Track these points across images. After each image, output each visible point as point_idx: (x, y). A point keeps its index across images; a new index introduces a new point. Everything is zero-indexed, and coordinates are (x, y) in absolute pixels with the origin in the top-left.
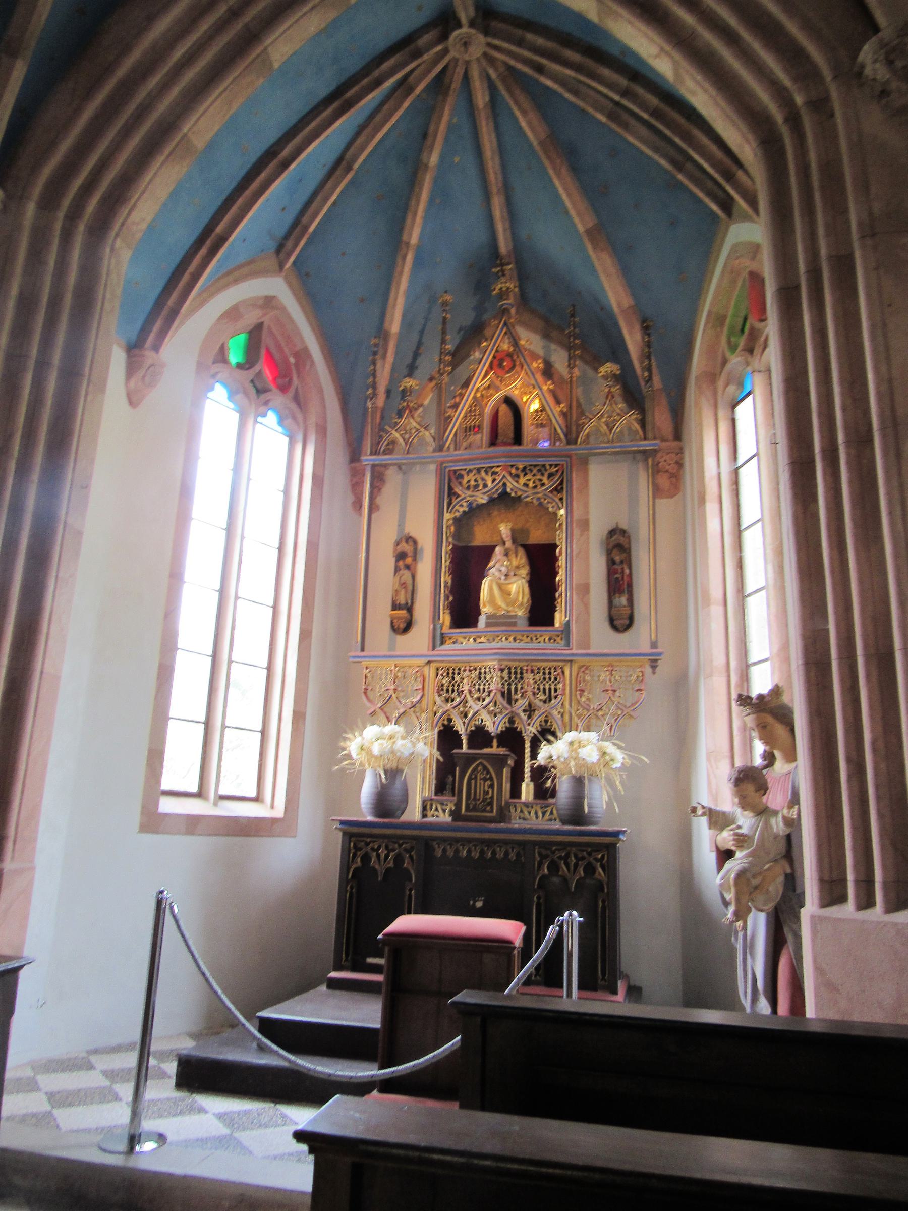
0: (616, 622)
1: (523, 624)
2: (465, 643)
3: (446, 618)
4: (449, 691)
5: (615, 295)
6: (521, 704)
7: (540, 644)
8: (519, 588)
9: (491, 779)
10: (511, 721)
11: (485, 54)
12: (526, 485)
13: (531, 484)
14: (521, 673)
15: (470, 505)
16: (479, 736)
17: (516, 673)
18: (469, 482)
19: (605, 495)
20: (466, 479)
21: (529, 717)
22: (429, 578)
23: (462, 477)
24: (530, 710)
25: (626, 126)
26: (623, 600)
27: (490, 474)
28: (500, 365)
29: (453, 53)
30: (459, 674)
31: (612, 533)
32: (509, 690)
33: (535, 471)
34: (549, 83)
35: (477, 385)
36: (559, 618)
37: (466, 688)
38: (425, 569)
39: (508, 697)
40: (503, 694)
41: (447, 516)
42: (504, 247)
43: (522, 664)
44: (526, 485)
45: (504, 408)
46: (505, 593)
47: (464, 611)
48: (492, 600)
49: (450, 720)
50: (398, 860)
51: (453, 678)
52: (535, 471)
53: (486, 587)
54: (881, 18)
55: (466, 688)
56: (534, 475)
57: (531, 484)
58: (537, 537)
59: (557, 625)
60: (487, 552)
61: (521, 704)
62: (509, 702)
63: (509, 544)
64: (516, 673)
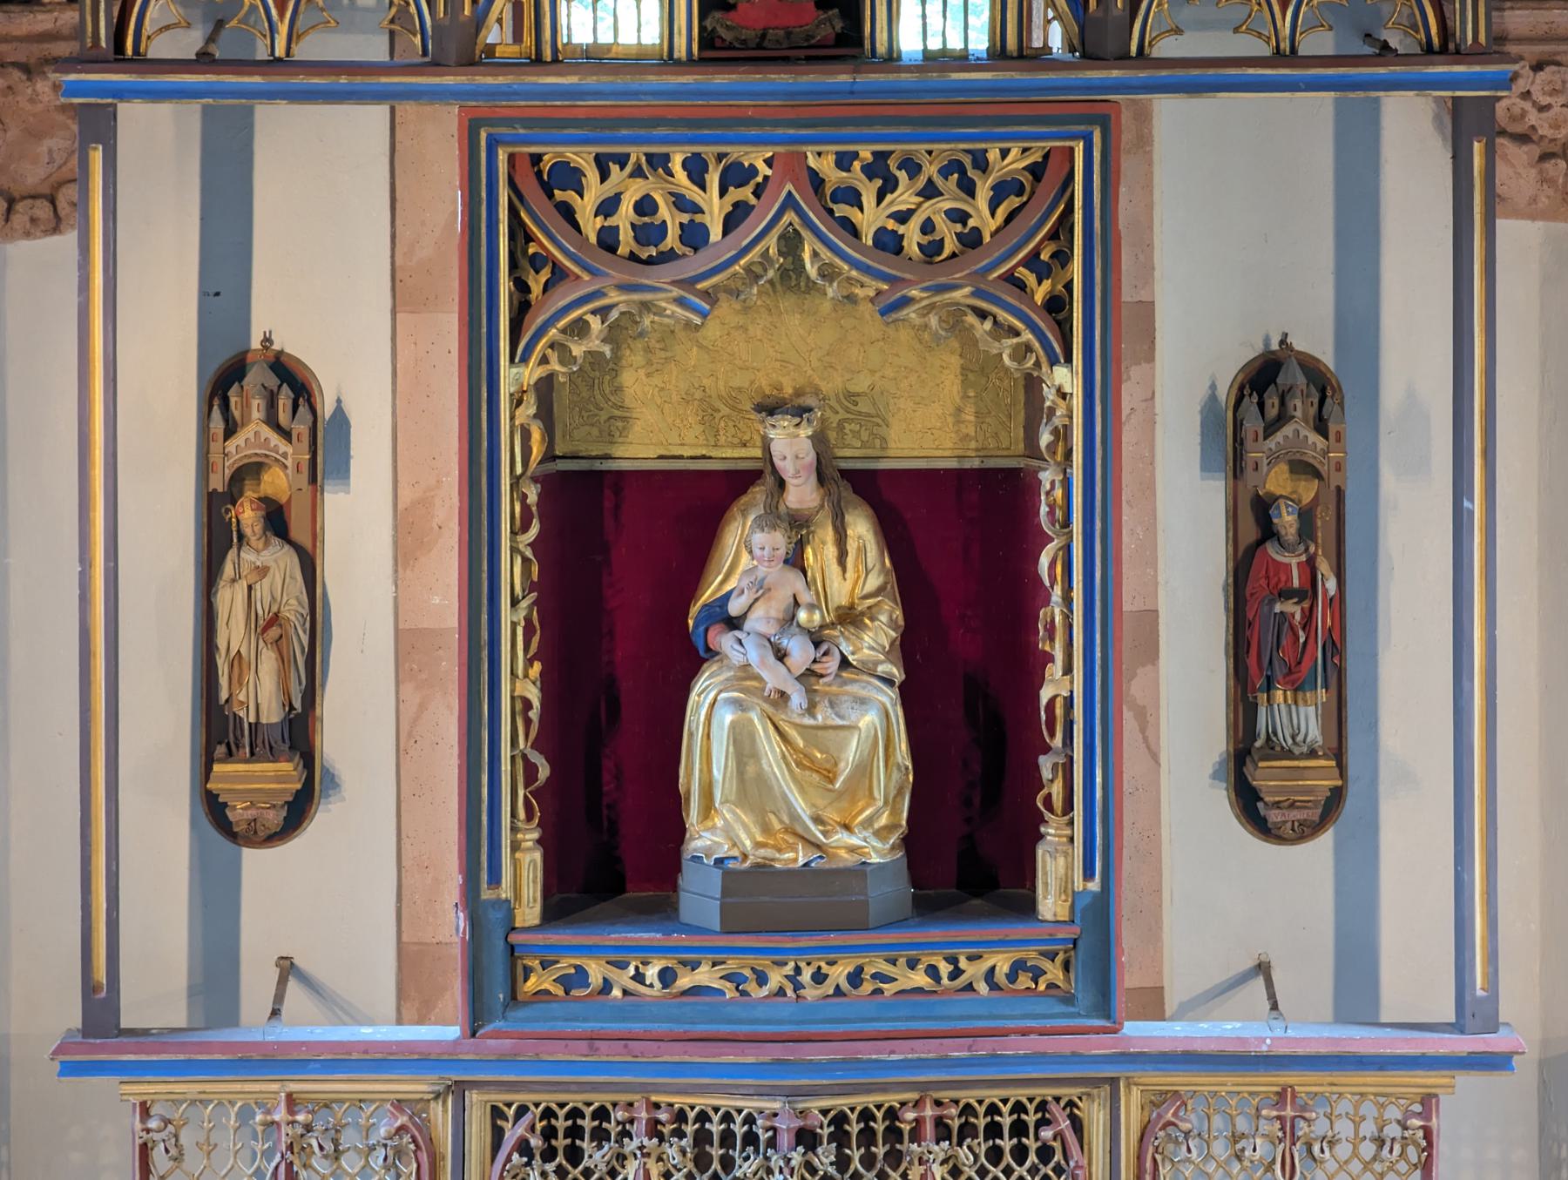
2: (622, 965)
3: (524, 872)
8: (870, 720)
12: (889, 243)
13: (912, 235)
14: (893, 1134)
17: (867, 1137)
18: (608, 207)
27: (713, 179)
30: (600, 1136)
33: (931, 170)
36: (1057, 872)
38: (356, 524)
41: (511, 377)
43: (892, 1099)
44: (889, 243)
46: (816, 767)
47: (604, 819)
48: (753, 790)
51: (574, 1155)
52: (931, 170)
56: (930, 191)
57: (912, 235)
59: (1051, 905)
60: (698, 504)
63: (802, 494)
64: (867, 1137)
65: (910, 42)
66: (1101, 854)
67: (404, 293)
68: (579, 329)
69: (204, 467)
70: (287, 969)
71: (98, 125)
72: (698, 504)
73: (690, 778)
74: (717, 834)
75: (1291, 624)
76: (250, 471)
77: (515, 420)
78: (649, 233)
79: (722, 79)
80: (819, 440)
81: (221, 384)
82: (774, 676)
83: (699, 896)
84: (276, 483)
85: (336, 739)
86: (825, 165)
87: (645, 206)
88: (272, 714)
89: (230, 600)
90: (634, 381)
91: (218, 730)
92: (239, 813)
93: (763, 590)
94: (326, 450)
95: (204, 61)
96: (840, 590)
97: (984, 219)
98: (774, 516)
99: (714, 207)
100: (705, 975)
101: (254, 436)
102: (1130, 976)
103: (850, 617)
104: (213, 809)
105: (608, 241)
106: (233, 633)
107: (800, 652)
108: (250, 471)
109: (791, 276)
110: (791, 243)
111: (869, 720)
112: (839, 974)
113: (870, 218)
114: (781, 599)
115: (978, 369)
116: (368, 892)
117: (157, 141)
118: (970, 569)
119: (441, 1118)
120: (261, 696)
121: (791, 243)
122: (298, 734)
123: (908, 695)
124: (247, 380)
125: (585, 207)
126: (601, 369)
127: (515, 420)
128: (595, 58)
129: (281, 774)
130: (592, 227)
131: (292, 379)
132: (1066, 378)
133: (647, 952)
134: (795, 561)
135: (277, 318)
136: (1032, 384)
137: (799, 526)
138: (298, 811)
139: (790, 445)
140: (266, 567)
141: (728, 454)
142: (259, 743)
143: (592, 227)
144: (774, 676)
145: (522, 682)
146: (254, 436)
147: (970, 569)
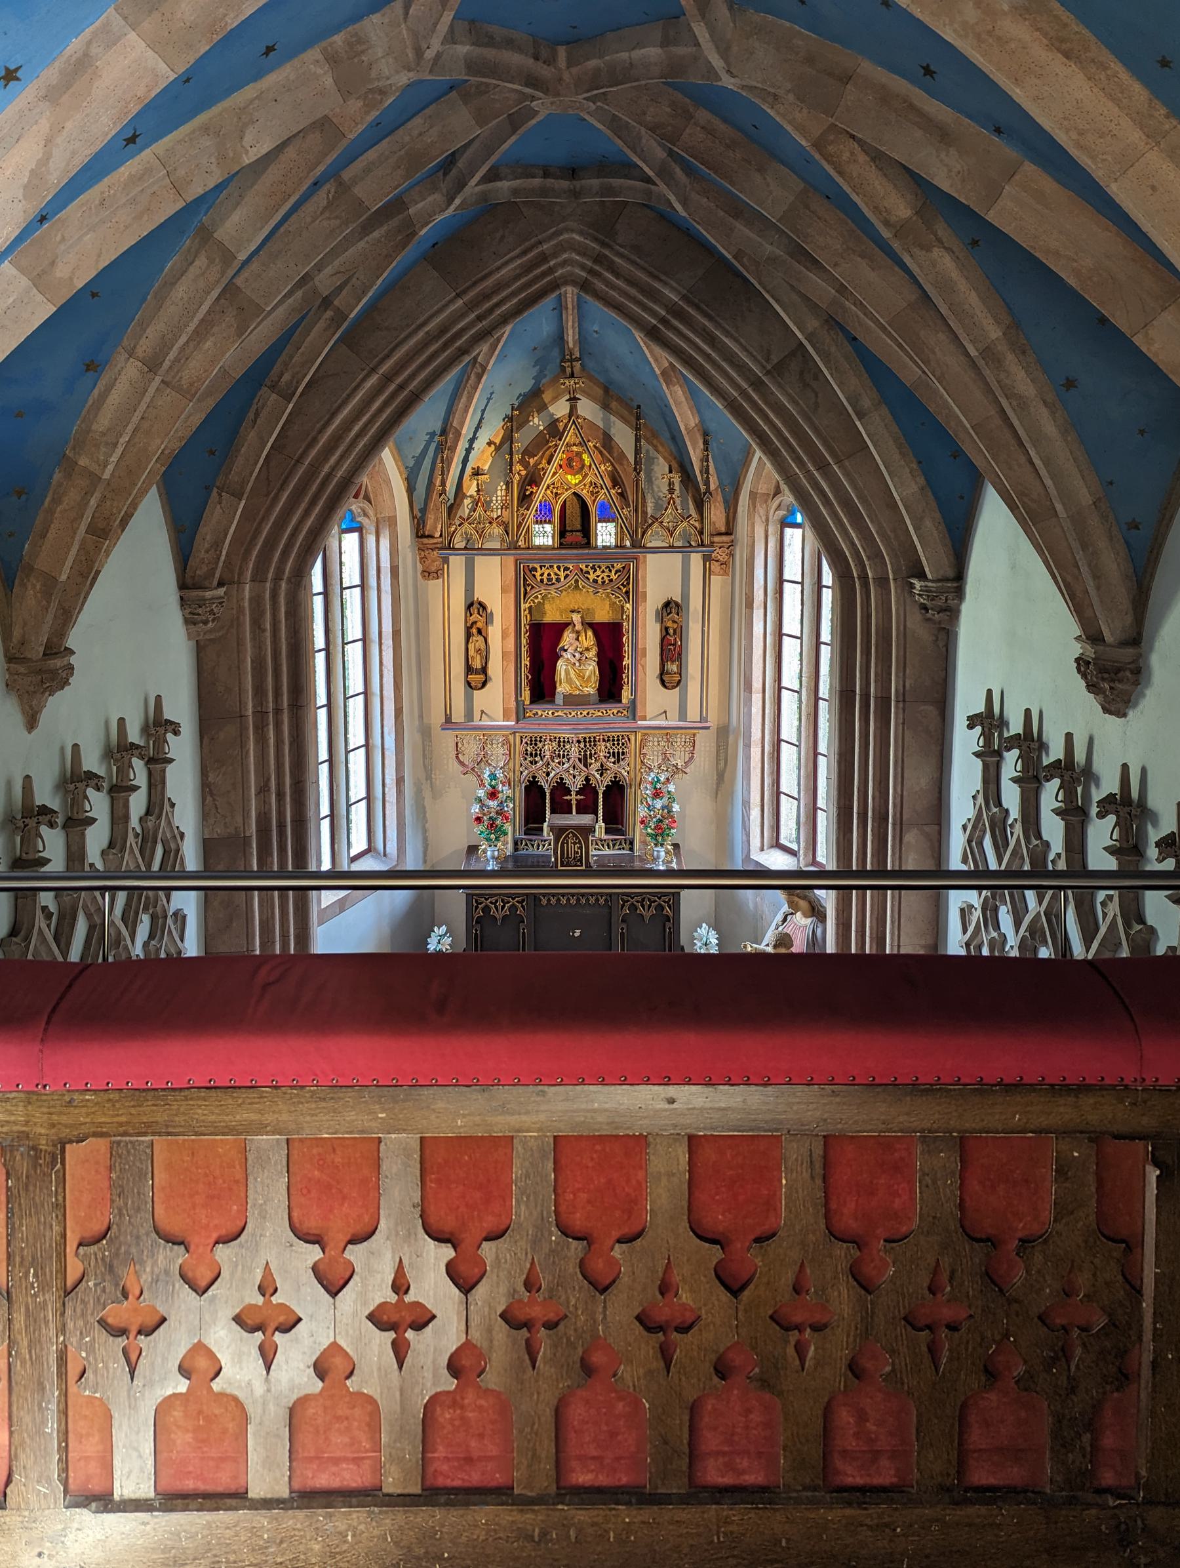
0: (666, 678)
2: (544, 711)
3: (526, 695)
4: (534, 755)
7: (609, 717)
8: (591, 668)
9: (580, 842)
10: (587, 779)
12: (595, 581)
13: (600, 580)
16: (561, 788)
18: (542, 575)
19: (660, 575)
20: (539, 572)
21: (601, 775)
24: (602, 770)
26: (675, 668)
31: (668, 605)
32: (585, 755)
35: (548, 482)
36: (626, 694)
37: (548, 753)
38: (495, 632)
39: (584, 761)
40: (580, 760)
44: (595, 581)
46: (581, 676)
47: (541, 685)
48: (569, 681)
49: (534, 777)
55: (548, 753)
57: (600, 580)
58: (603, 615)
59: (624, 701)
62: (586, 766)
63: (579, 627)
65: (599, 543)
66: (634, 691)
67: (504, 590)
68: (537, 597)
69: (466, 622)
70: (482, 712)
71: (446, 560)
73: (557, 678)
74: (562, 688)
76: (475, 623)
77: (524, 614)
78: (550, 580)
79: (563, 552)
80: (582, 617)
81: (469, 607)
82: (573, 660)
83: (559, 699)
84: (479, 625)
85: (490, 672)
86: (583, 567)
87: (549, 575)
88: (479, 667)
90: (547, 606)
91: (469, 669)
92: (473, 684)
93: (571, 644)
94: (489, 619)
95: (466, 548)
96: (586, 644)
97: (614, 577)
98: (573, 631)
99: (562, 574)
100: (560, 713)
101: (475, 616)
102: (639, 714)
103: (587, 649)
104: (469, 684)
105: (542, 581)
106: (472, 652)
107: (577, 655)
108: (475, 623)
109: (577, 587)
110: (577, 581)
111: (591, 668)
112: (585, 713)
113: (592, 577)
114: (573, 648)
115: (613, 604)
116: (497, 699)
117: (457, 563)
118: (610, 641)
119: (511, 738)
120: (477, 664)
121: (577, 581)
122: (484, 670)
123: (598, 663)
124: (474, 606)
125: (538, 574)
126: (540, 605)
127: (524, 614)
128: (539, 547)
129: (481, 677)
130: (539, 578)
131: (482, 606)
133: (549, 709)
134: (577, 639)
135: (479, 595)
136: (623, 607)
137: (578, 632)
138: (484, 684)
139: (576, 618)
140: (477, 641)
141: (564, 620)
142: (477, 672)
143: (539, 578)
144: (573, 660)
145: (526, 661)
146: (475, 616)
147: (610, 641)
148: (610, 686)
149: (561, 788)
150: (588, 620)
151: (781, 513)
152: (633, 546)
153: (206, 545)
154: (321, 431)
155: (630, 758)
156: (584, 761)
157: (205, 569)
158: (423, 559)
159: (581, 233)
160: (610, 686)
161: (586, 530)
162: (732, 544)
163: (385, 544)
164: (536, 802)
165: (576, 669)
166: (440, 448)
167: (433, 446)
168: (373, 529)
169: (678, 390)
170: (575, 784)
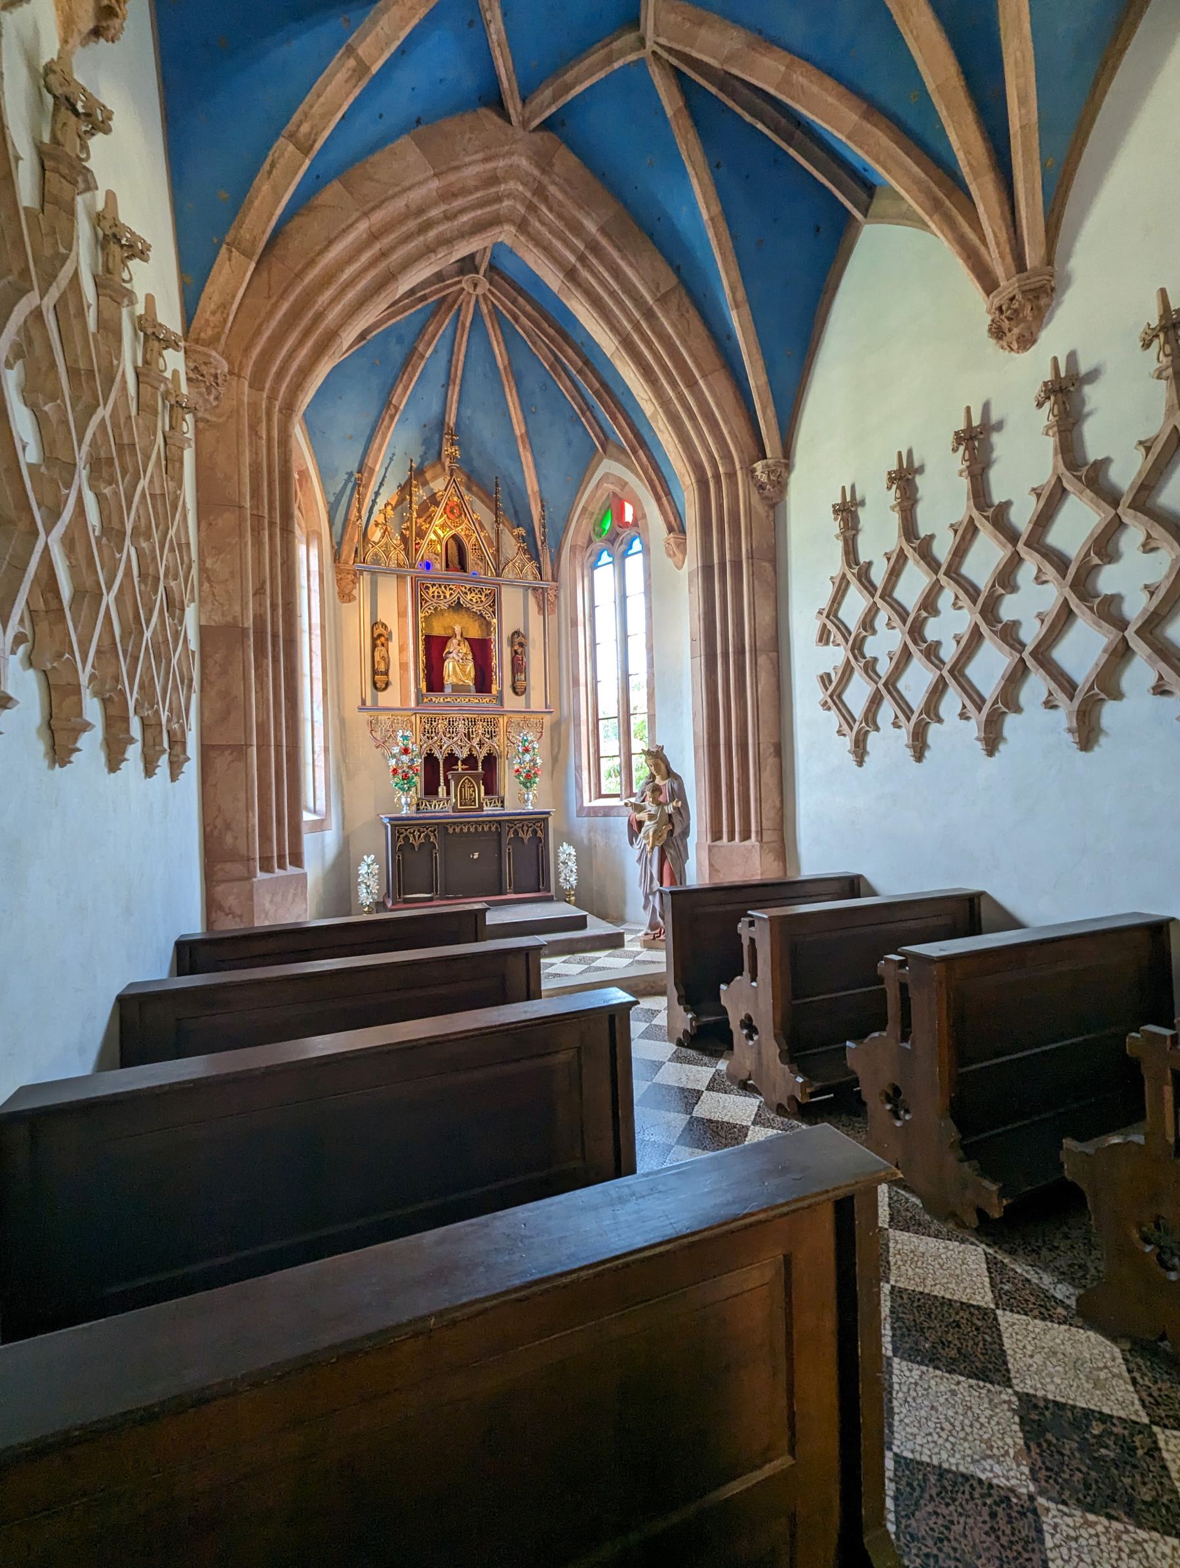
1: (473, 688)
3: (423, 685)
4: (429, 733)
5: (531, 485)
6: (475, 742)
8: (470, 667)
10: (470, 750)
11: (484, 295)
15: (436, 609)
16: (451, 759)
22: (404, 655)
23: (427, 588)
24: (481, 744)
25: (559, 376)
26: (523, 677)
28: (452, 512)
29: (464, 285)
34: (520, 331)
36: (495, 688)
38: (394, 646)
39: (468, 736)
42: (451, 420)
45: (452, 543)
46: (463, 671)
47: (434, 681)
50: (427, 836)
53: (449, 666)
54: (769, 454)
58: (475, 632)
59: (494, 692)
60: (444, 641)
61: (475, 742)
63: (459, 637)
72: (444, 641)
75: (518, 666)
81: (374, 624)
83: (448, 690)
89: (377, 654)
91: (375, 672)
104: (374, 684)
106: (377, 658)
108: (380, 635)
113: (469, 597)
118: (481, 650)
120: (382, 668)
122: (386, 673)
131: (385, 626)
132: (495, 621)
135: (381, 617)
138: (387, 684)
142: (382, 673)
147: (481, 650)
148: (483, 682)
149: (451, 759)
150: (465, 635)
151: (592, 559)
152: (498, 575)
153: (213, 306)
154: (321, 252)
155: (501, 737)
156: (468, 736)
157: (210, 332)
158: (339, 581)
159: (529, 158)
160: (483, 682)
161: (463, 567)
162: (557, 589)
163: (314, 552)
164: (433, 772)
165: (458, 667)
166: (357, 485)
167: (350, 485)
168: (304, 540)
169: (529, 455)
170: (462, 754)
